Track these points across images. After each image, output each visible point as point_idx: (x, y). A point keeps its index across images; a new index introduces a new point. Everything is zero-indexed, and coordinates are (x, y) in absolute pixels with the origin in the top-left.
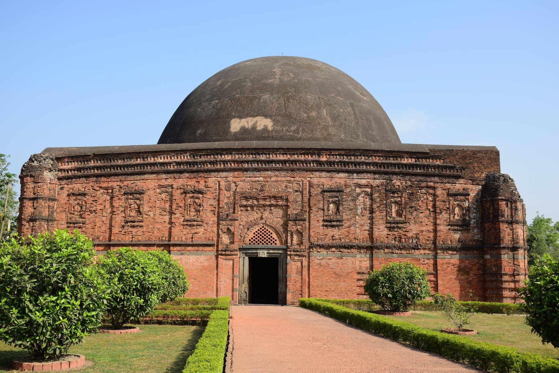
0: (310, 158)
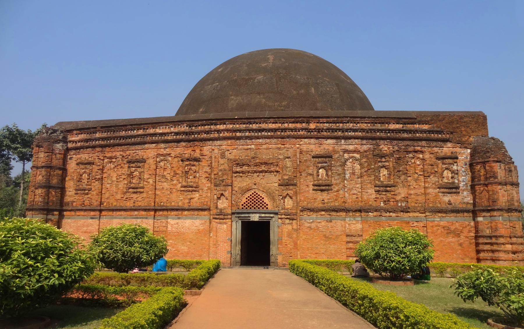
0: (299, 126)
